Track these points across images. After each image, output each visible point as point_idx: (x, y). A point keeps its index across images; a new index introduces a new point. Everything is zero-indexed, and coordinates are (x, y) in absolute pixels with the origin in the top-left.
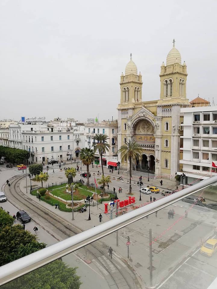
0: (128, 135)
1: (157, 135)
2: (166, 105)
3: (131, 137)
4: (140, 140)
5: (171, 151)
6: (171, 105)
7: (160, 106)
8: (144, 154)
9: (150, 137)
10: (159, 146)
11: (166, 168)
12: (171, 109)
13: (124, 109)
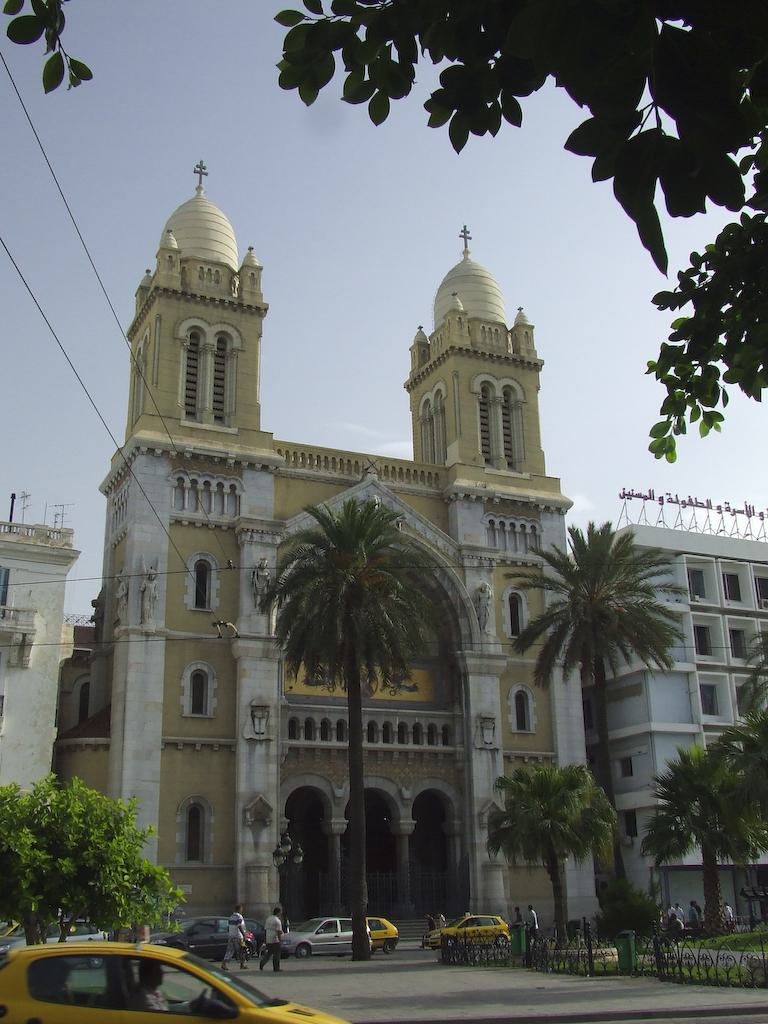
0: (259, 645)
7: (479, 498)
10: (498, 723)
13: (210, 459)
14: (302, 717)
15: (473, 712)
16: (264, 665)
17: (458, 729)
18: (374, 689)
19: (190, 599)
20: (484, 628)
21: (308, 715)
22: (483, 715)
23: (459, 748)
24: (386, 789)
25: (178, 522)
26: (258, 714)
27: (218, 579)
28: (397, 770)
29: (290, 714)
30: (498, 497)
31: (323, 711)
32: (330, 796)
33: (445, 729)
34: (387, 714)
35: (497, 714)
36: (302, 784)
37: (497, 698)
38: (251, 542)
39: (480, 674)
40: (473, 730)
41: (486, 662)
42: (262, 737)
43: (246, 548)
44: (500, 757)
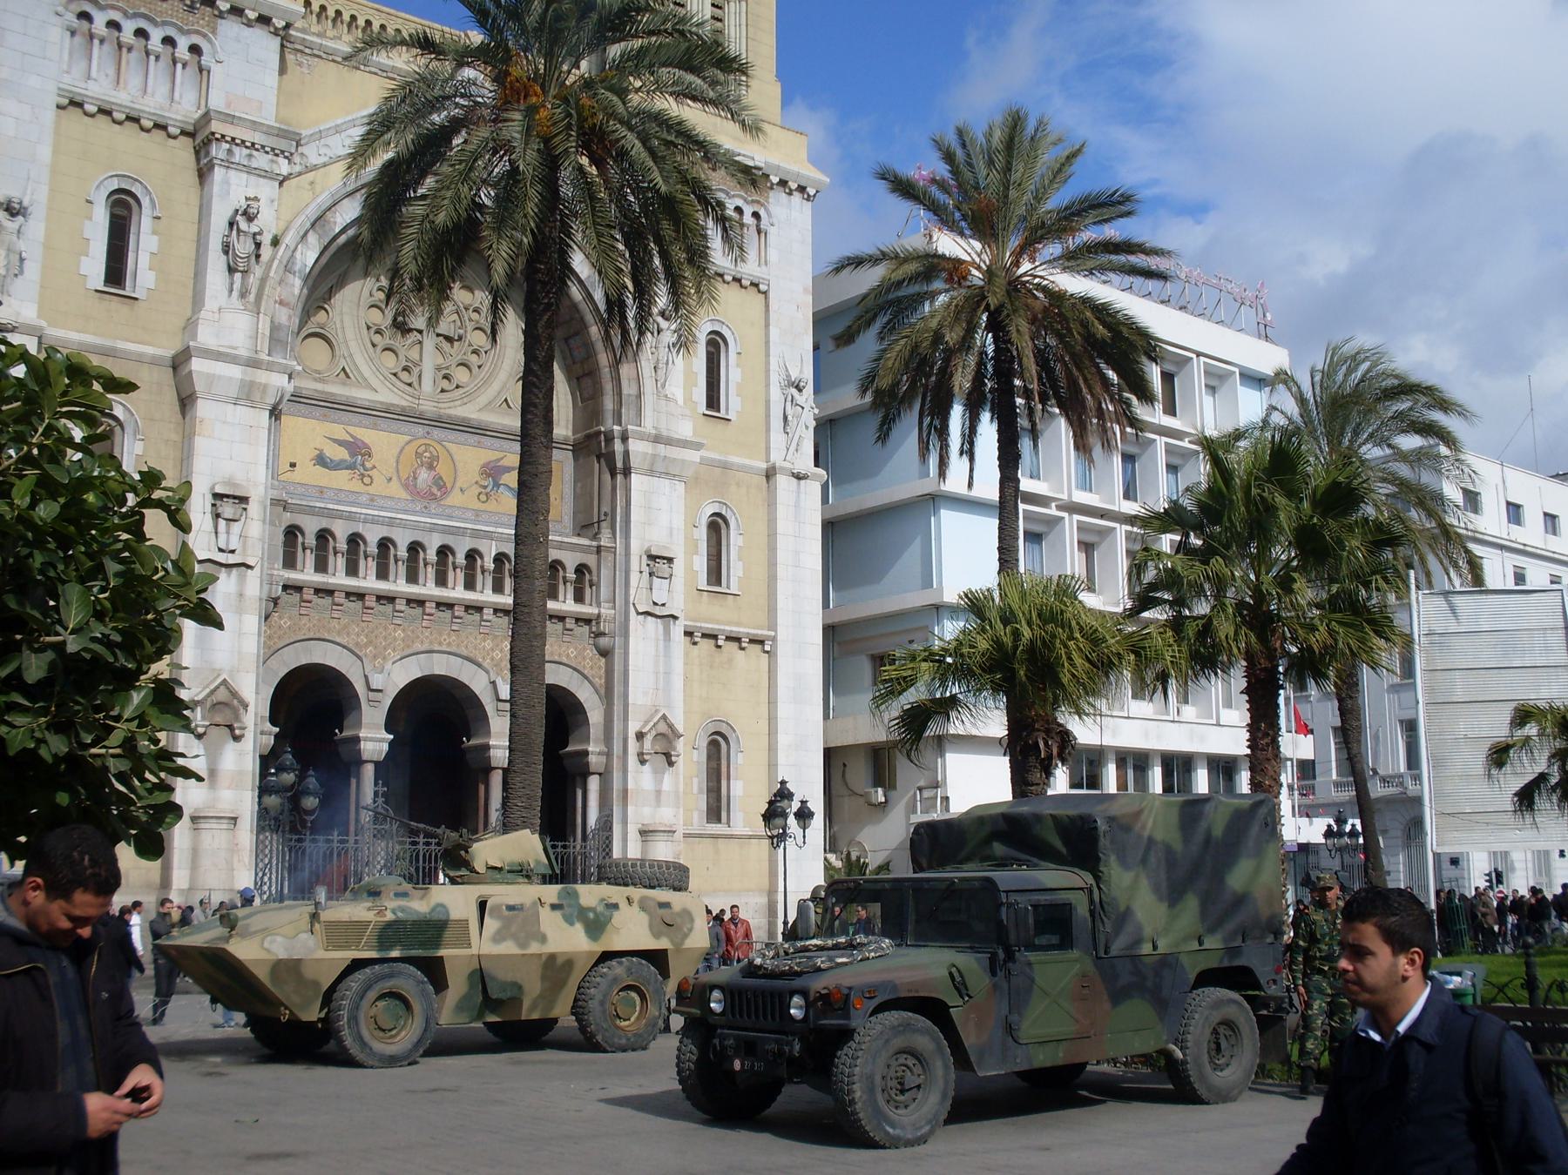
0: (235, 372)
1: (669, 442)
4: (341, 479)
8: (441, 666)
9: (491, 456)
10: (678, 565)
14: (311, 526)
15: (636, 547)
16: (242, 413)
17: (605, 573)
19: (95, 266)
20: (663, 386)
21: (324, 523)
22: (654, 553)
23: (606, 611)
24: (464, 678)
25: (76, 104)
26: (228, 509)
27: (154, 233)
28: (488, 644)
29: (288, 518)
31: (350, 517)
32: (360, 687)
33: (581, 570)
34: (476, 534)
35: (678, 551)
36: (304, 660)
37: (679, 521)
38: (229, 164)
39: (651, 472)
40: (634, 578)
41: (662, 449)
42: (231, 559)
43: (218, 173)
44: (677, 630)
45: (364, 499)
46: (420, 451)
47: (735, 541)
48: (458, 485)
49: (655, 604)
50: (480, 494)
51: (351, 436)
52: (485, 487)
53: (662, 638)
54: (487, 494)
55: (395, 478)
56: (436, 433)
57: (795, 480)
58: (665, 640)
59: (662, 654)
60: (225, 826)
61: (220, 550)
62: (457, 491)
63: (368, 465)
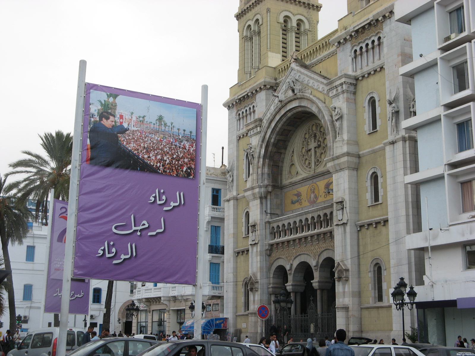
2: (363, 28)
3: (261, 198)
5: (391, 216)
6: (377, 20)
7: (345, 39)
8: (303, 259)
11: (379, 304)
12: (379, 38)
18: (318, 196)
28: (312, 248)
30: (352, 32)
36: (278, 265)
39: (337, 171)
41: (337, 162)
45: (301, 209)
46: (311, 188)
47: (380, 180)
48: (320, 195)
49: (339, 220)
50: (325, 195)
51: (298, 191)
52: (326, 192)
53: (343, 232)
54: (326, 195)
55: (306, 200)
56: (315, 180)
57: (392, 146)
58: (344, 233)
59: (343, 239)
60: (254, 315)
61: (253, 241)
62: (320, 196)
63: (301, 199)
